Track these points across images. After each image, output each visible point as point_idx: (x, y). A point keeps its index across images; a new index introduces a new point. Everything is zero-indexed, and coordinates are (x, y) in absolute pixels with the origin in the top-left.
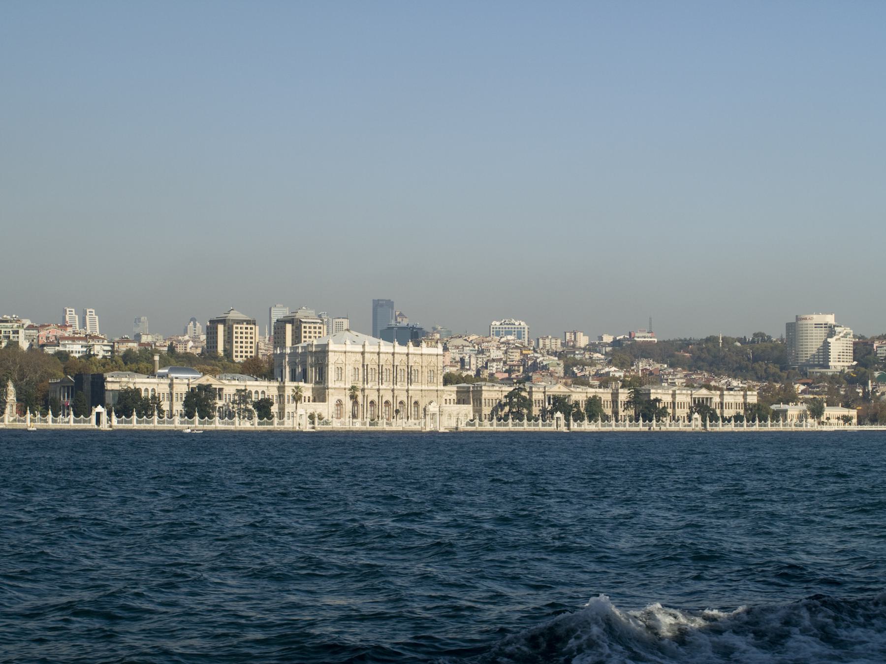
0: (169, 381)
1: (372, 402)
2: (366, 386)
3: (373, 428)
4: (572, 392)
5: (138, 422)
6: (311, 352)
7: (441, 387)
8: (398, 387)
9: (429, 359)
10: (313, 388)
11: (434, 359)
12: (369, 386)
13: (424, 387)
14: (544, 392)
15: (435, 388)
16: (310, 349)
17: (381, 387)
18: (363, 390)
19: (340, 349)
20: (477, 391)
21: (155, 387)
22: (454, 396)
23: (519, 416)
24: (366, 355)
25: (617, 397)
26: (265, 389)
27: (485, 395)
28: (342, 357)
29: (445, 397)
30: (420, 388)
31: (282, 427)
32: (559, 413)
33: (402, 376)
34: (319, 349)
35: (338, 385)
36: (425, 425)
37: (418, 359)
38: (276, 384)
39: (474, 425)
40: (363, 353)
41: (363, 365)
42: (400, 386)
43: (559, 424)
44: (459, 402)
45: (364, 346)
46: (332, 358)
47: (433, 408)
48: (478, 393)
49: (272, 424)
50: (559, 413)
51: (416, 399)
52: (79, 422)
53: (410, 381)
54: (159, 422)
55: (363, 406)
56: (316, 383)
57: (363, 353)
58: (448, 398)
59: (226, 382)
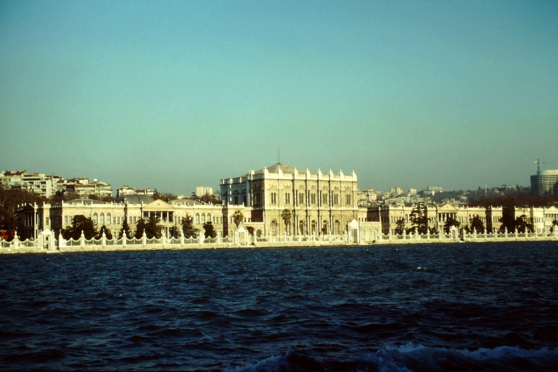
0: (124, 207)
2: (296, 208)
4: (457, 210)
6: (250, 181)
10: (252, 211)
12: (299, 208)
14: (437, 211)
16: (249, 178)
17: (308, 208)
18: (294, 211)
20: (385, 210)
21: (110, 211)
22: (365, 215)
24: (295, 182)
25: (490, 214)
27: (391, 214)
28: (276, 183)
30: (340, 209)
31: (224, 245)
32: (453, 227)
34: (255, 178)
35: (272, 208)
38: (220, 207)
41: (293, 191)
44: (369, 219)
45: (293, 175)
46: (267, 185)
48: (386, 212)
50: (453, 227)
51: (337, 219)
54: (107, 243)
56: (254, 206)
57: (293, 181)
59: (176, 206)
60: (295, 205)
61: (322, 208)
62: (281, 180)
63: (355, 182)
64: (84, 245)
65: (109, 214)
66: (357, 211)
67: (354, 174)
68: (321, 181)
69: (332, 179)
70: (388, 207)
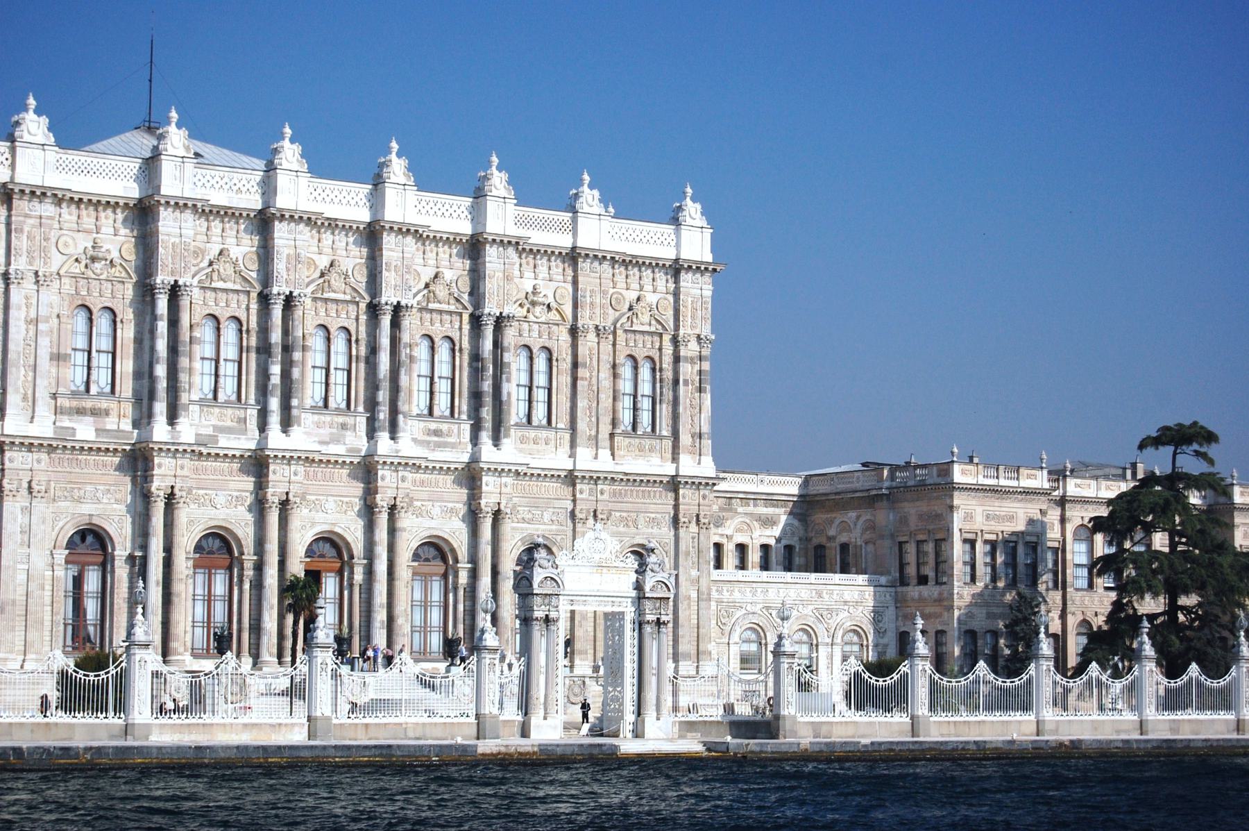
3: (87, 730)
9: (627, 288)
11: (656, 291)
12: (187, 430)
13: (586, 460)
29: (732, 532)
37: (551, 282)
39: (896, 698)
42: (425, 440)
47: (591, 577)
53: (484, 407)
60: (160, 408)
62: (37, 194)
63: (698, 268)
67: (693, 211)
68: (404, 231)
70: (945, 470)
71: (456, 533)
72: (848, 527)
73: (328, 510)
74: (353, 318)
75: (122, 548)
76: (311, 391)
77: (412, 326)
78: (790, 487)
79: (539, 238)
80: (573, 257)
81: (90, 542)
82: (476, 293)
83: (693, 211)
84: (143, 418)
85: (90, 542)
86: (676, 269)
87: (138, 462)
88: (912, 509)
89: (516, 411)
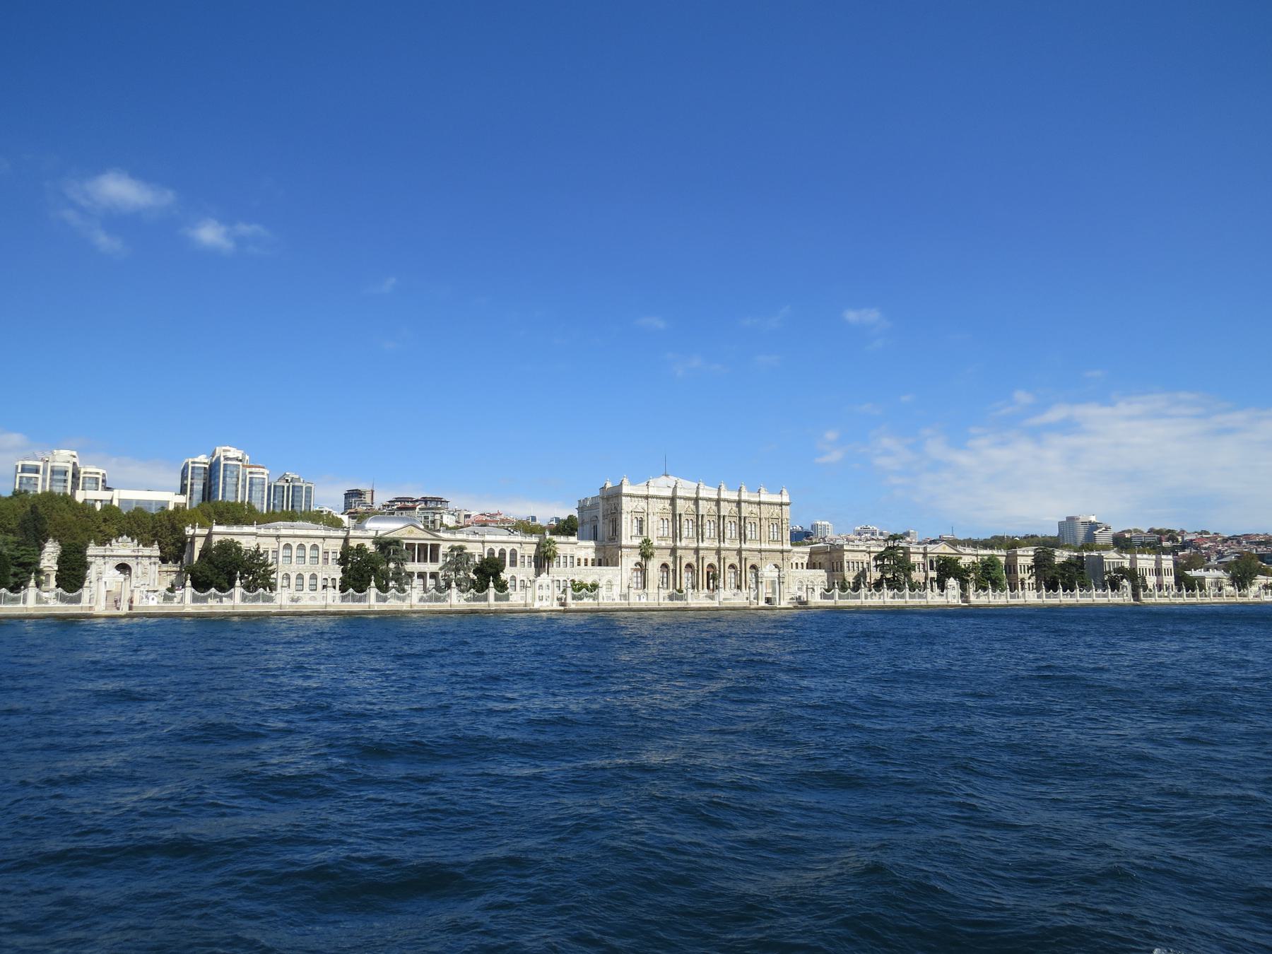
1: (689, 566)
2: (678, 544)
5: (244, 599)
7: (787, 546)
8: (727, 545)
15: (778, 547)
17: (701, 545)
19: (640, 493)
23: (894, 584)
26: (516, 547)
28: (642, 504)
29: (794, 560)
31: (504, 605)
33: (731, 530)
36: (757, 598)
37: (755, 509)
39: (832, 597)
40: (673, 500)
43: (952, 595)
47: (768, 572)
49: (486, 598)
52: (256, 599)
55: (675, 571)
57: (673, 500)
58: (799, 562)
61: (727, 545)
62: (653, 497)
64: (235, 601)
65: (315, 547)
66: (789, 551)
68: (725, 500)
69: (745, 496)
71: (736, 561)
72: (820, 559)
73: (711, 558)
74: (715, 518)
75: (671, 567)
76: (707, 535)
77: (727, 520)
78: (807, 549)
79: (752, 499)
80: (759, 503)
81: (665, 566)
82: (740, 511)
83: (785, 492)
84: (674, 540)
85: (665, 566)
86: (781, 504)
87: (674, 551)
88: (835, 555)
89: (749, 537)
